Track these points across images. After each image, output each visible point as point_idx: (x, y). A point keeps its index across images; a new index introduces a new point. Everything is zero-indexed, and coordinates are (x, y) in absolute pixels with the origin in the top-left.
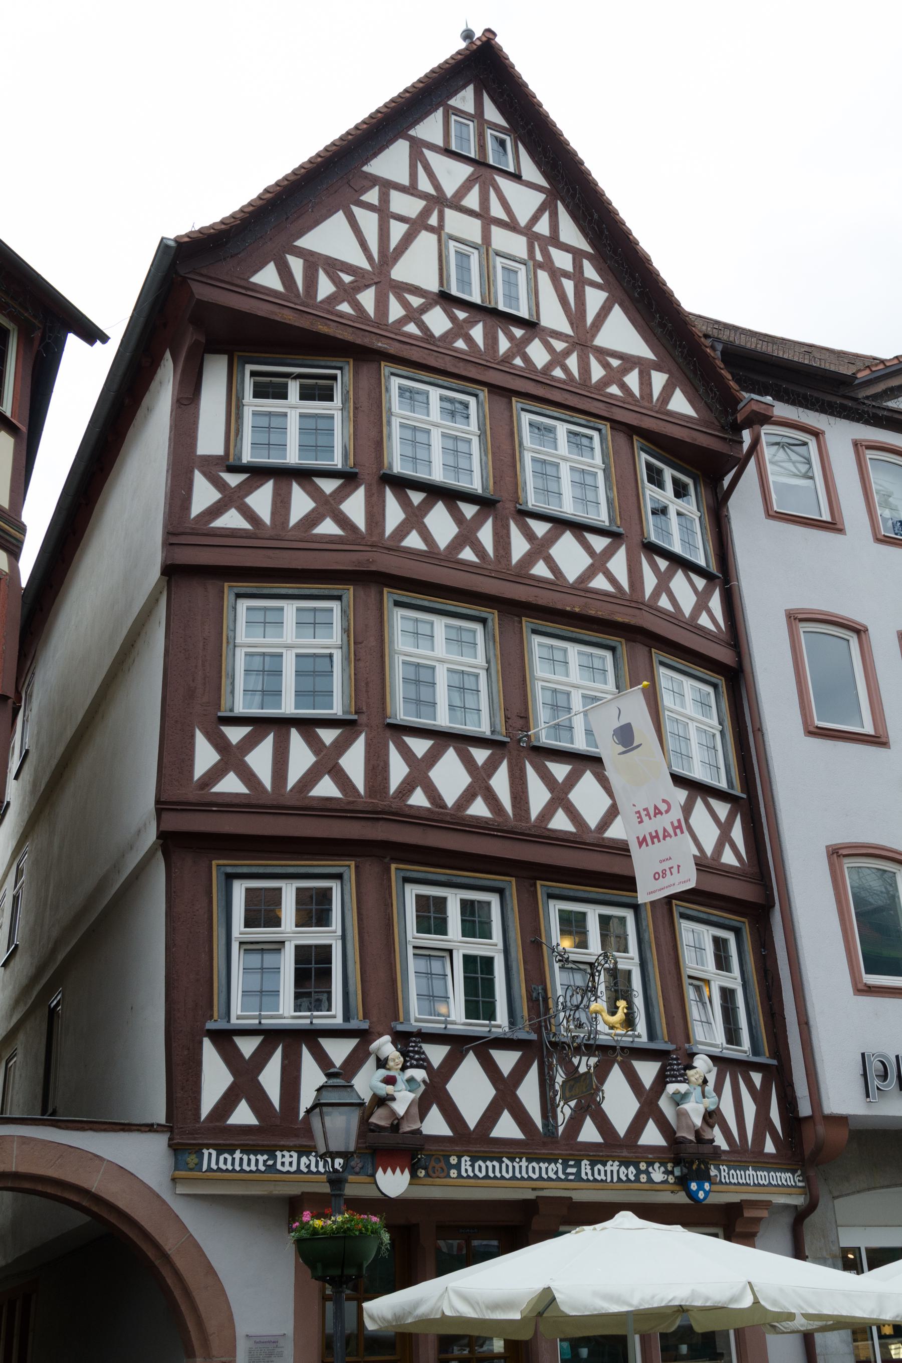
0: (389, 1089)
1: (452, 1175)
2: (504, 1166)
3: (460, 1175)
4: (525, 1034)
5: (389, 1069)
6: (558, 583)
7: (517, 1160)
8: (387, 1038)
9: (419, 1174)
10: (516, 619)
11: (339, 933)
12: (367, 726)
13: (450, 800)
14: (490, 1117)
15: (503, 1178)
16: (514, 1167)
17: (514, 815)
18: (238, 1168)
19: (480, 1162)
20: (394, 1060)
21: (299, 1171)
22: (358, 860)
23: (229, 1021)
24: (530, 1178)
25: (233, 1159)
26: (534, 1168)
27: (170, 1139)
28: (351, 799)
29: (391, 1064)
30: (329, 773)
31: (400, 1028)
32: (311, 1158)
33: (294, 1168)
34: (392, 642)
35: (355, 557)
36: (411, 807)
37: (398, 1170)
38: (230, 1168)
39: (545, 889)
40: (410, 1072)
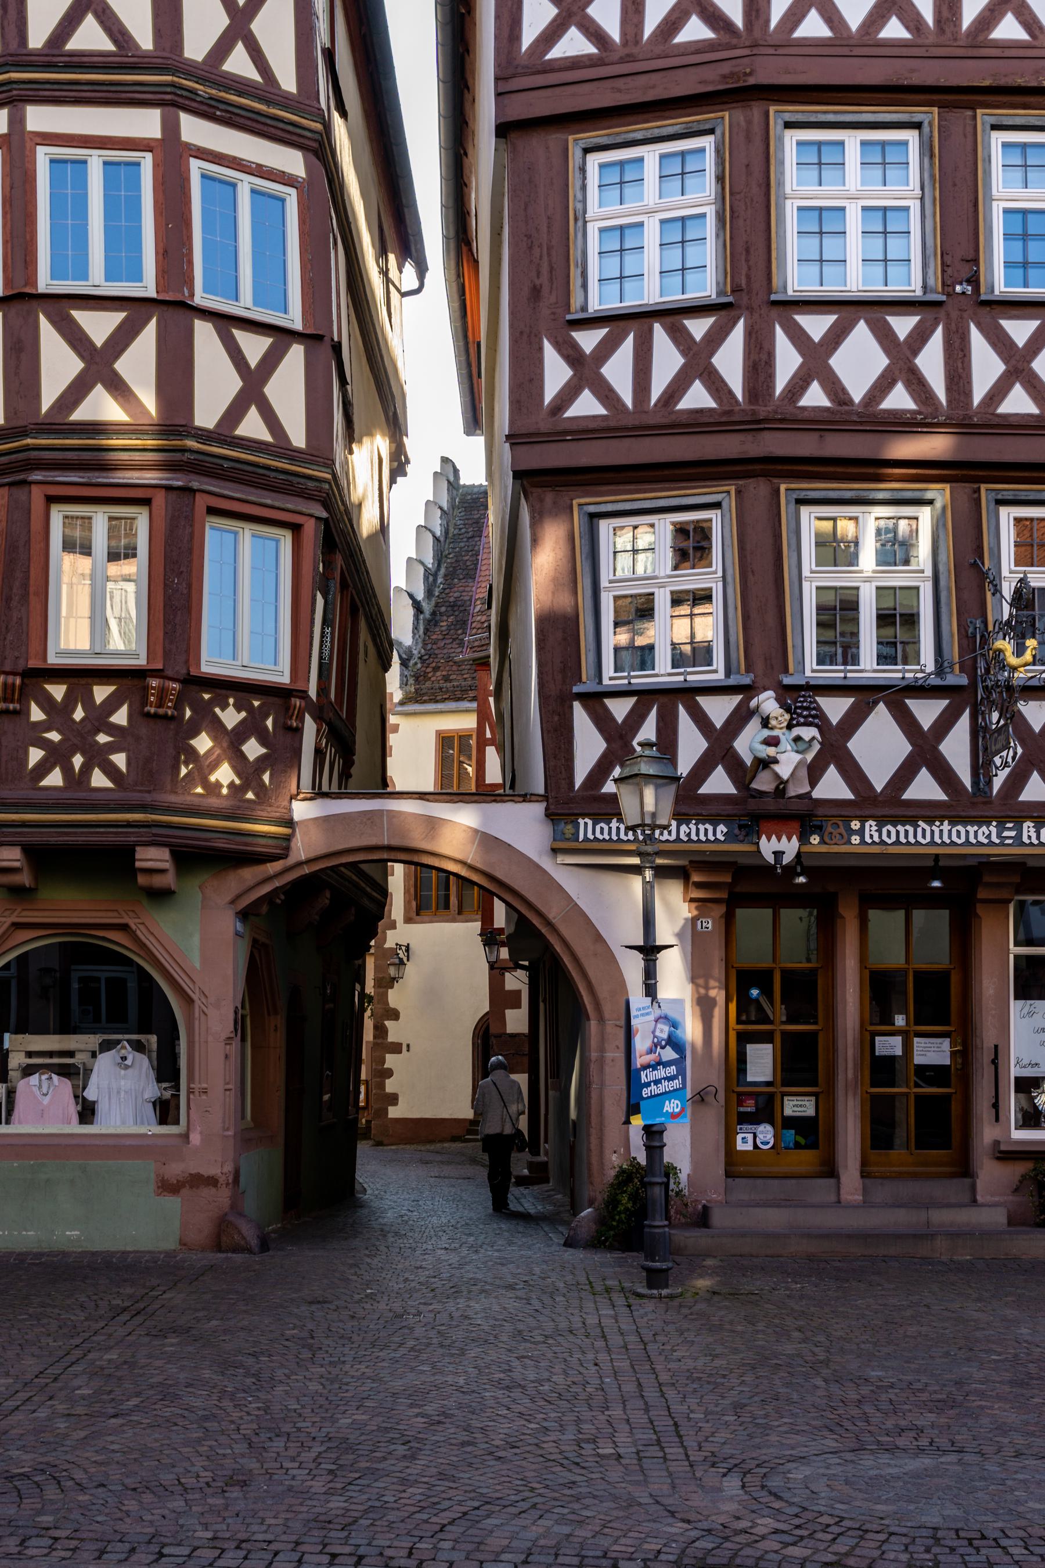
0: (771, 751)
1: (853, 842)
2: (919, 830)
3: (863, 842)
4: (957, 678)
5: (772, 729)
6: (1036, 43)
7: (937, 823)
8: (770, 693)
9: (812, 840)
10: (969, 113)
11: (720, 574)
12: (747, 308)
13: (857, 395)
14: (904, 775)
15: (918, 843)
16: (932, 832)
17: (949, 401)
18: (615, 838)
19: (890, 827)
20: (777, 718)
21: (678, 840)
22: (740, 482)
23: (600, 682)
24: (953, 843)
25: (610, 828)
26: (958, 832)
27: (547, 809)
28: (727, 408)
29: (773, 722)
30: (700, 376)
31: (787, 681)
32: (691, 826)
33: (674, 837)
34: (781, 184)
35: (726, 68)
36: (804, 408)
37: (784, 838)
38: (607, 838)
39: (993, 494)
40: (797, 731)
